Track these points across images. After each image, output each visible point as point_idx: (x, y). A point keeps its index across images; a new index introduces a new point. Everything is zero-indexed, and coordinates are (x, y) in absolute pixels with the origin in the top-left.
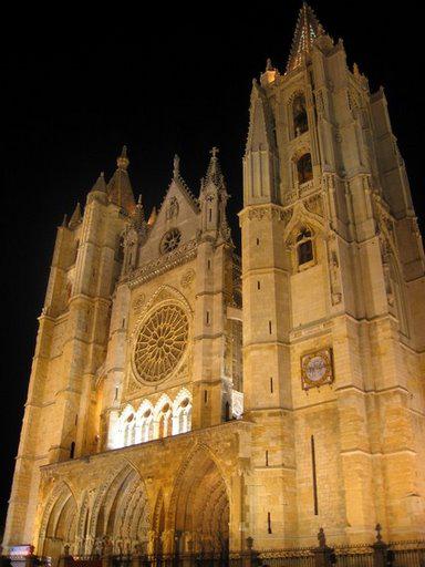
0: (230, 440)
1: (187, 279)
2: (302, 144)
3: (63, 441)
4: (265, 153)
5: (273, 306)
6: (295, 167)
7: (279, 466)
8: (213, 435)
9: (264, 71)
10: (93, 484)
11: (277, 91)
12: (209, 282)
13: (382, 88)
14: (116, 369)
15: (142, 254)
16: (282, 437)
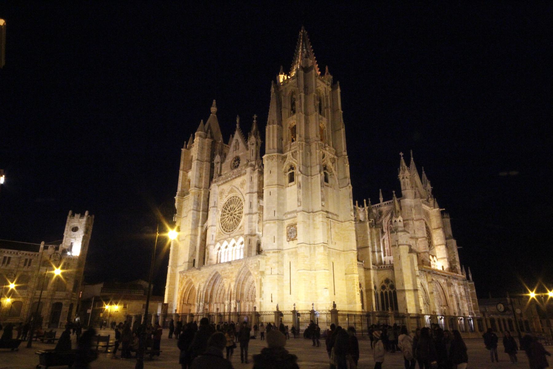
0: (257, 263)
1: (242, 184)
2: (292, 121)
3: (189, 259)
4: (275, 126)
5: (276, 203)
6: (290, 131)
7: (276, 275)
8: (250, 261)
9: (278, 74)
10: (203, 280)
11: (282, 88)
12: (251, 187)
13: (338, 83)
14: (212, 226)
15: (223, 168)
16: (278, 262)
